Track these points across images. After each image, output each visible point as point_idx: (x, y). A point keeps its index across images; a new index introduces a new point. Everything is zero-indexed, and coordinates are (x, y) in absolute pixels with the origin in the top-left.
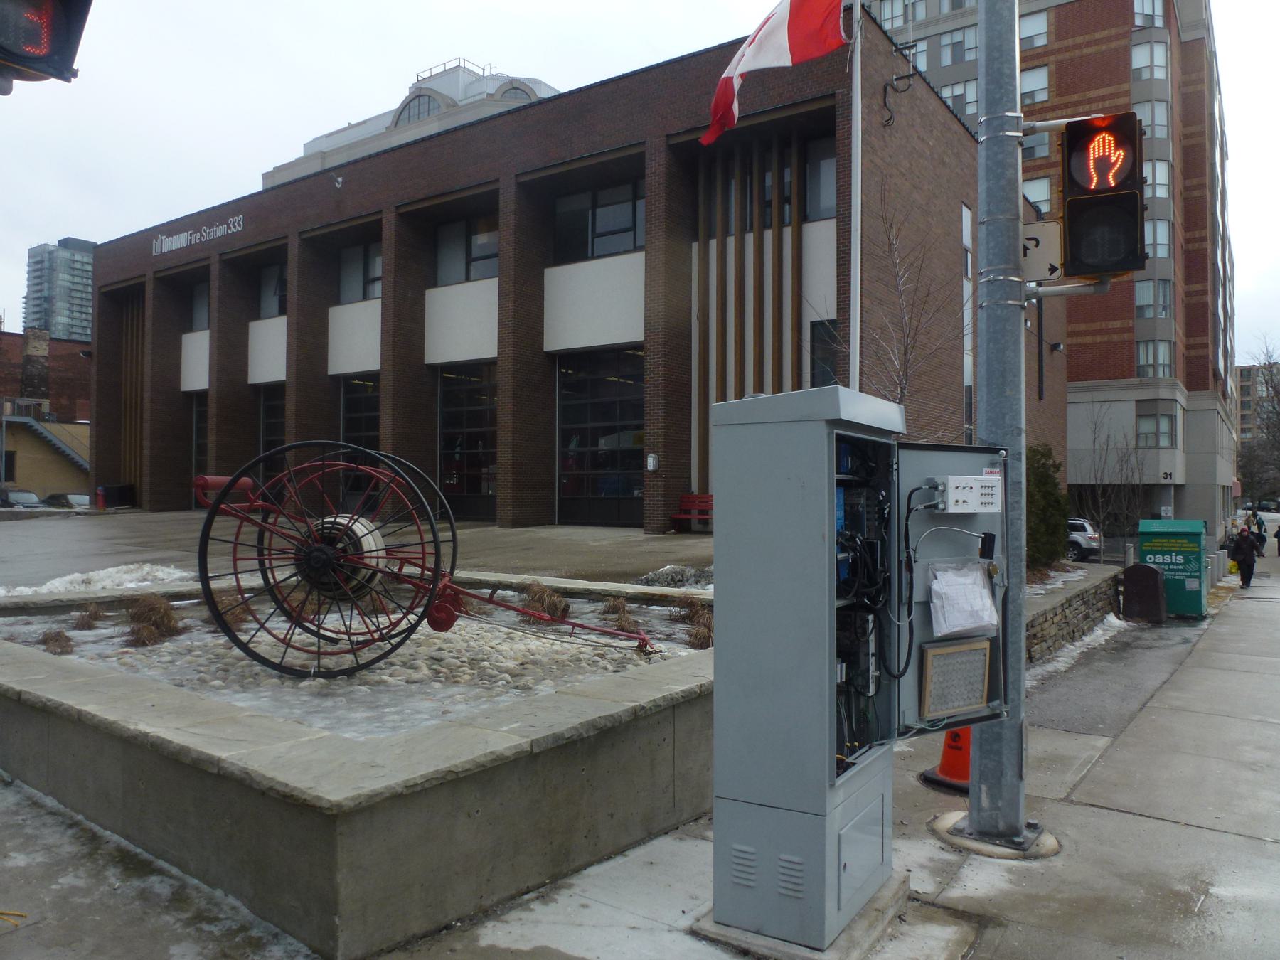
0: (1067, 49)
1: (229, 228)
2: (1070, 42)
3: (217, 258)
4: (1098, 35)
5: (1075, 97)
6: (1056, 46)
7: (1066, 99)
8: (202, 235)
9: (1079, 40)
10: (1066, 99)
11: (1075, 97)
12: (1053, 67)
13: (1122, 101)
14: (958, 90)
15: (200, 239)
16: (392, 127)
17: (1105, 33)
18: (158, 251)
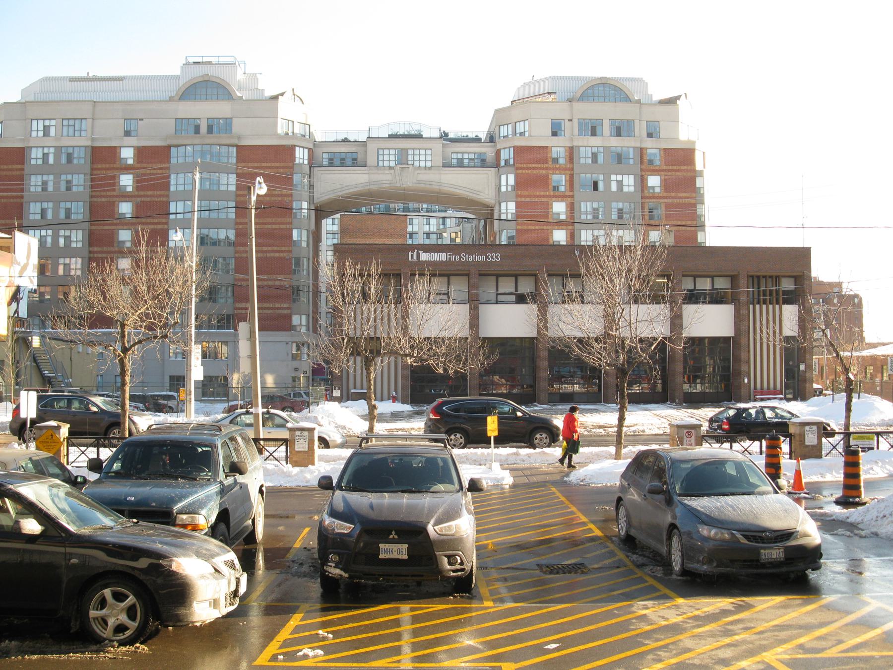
0: (669, 170)
1: (487, 257)
2: (670, 167)
3: (477, 272)
4: (683, 168)
5: (673, 195)
6: (665, 167)
7: (669, 195)
8: (460, 257)
9: (675, 167)
10: (669, 195)
11: (673, 195)
12: (663, 177)
13: (692, 201)
14: (619, 177)
15: (460, 259)
16: (177, 98)
17: (685, 168)
18: (415, 258)
